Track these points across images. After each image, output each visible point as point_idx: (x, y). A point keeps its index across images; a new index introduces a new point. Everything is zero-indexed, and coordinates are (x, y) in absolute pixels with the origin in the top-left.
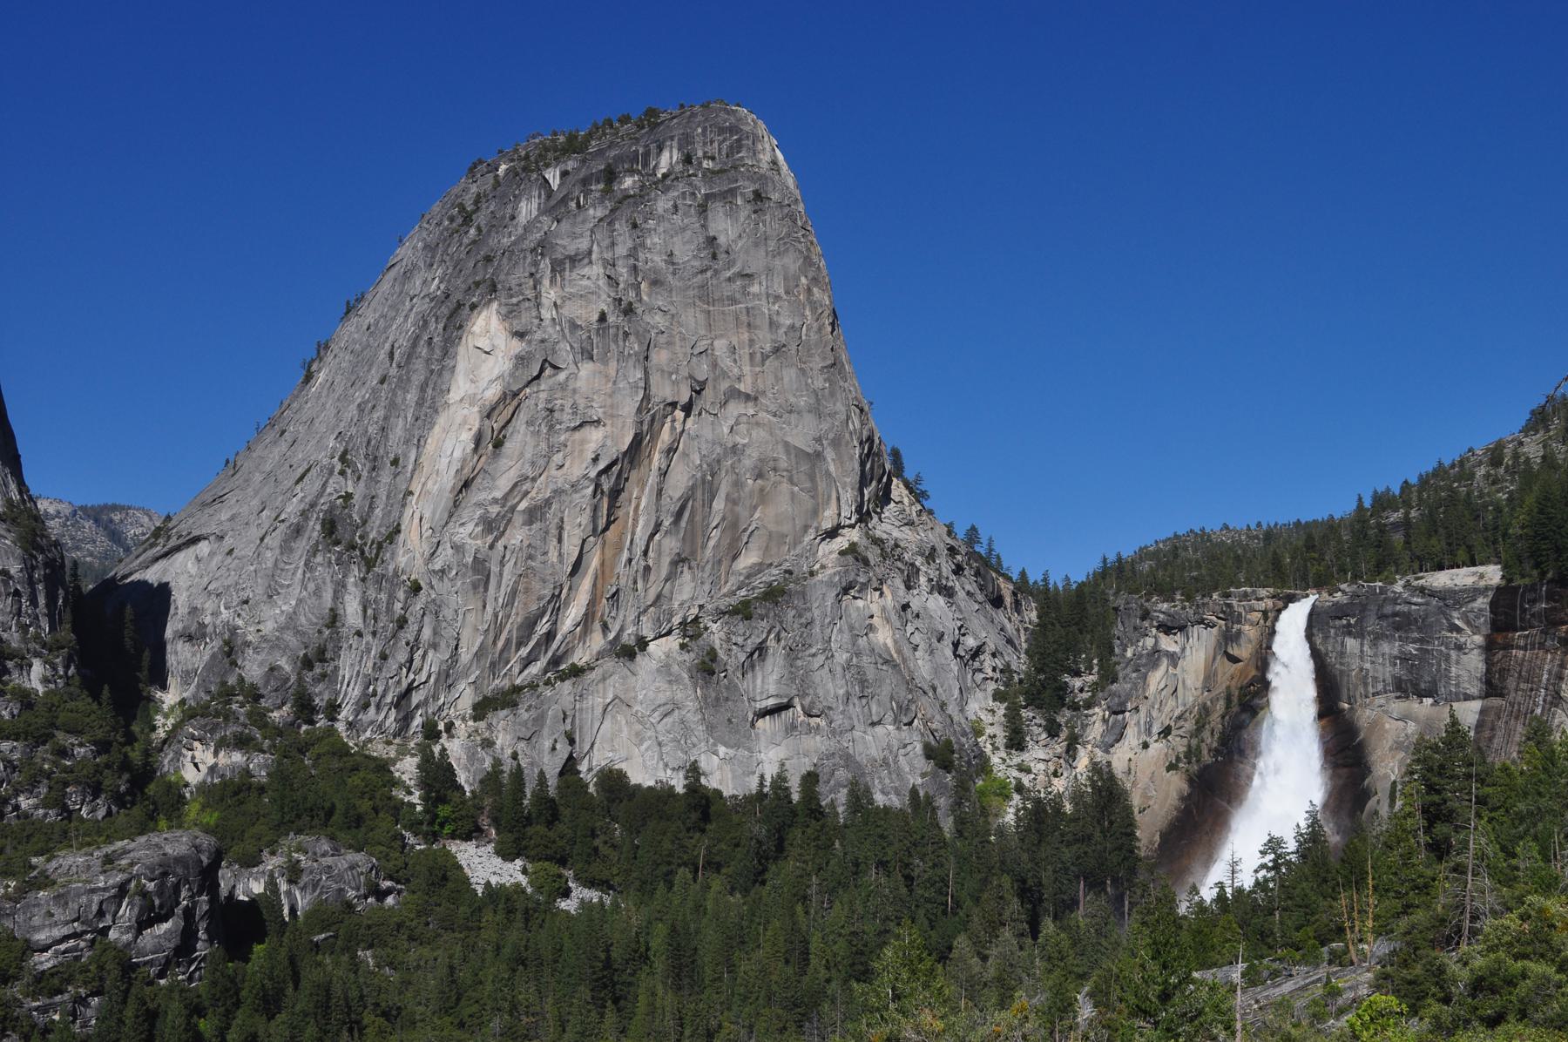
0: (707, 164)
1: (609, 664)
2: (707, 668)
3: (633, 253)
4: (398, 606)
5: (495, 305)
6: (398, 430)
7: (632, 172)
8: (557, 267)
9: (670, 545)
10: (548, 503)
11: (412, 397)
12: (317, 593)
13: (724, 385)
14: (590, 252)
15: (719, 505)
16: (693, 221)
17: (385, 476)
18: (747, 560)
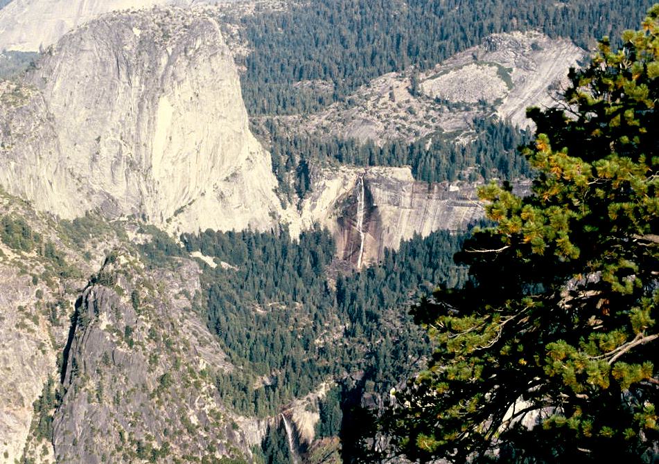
0: (208, 43)
1: (201, 198)
2: (221, 196)
3: (197, 79)
4: (155, 189)
5: (165, 97)
6: (143, 135)
7: (191, 48)
8: (179, 83)
9: (210, 164)
10: (187, 156)
11: (146, 124)
12: (134, 184)
13: (219, 115)
14: (186, 78)
15: (220, 150)
16: (208, 64)
17: (143, 149)
18: (227, 164)
